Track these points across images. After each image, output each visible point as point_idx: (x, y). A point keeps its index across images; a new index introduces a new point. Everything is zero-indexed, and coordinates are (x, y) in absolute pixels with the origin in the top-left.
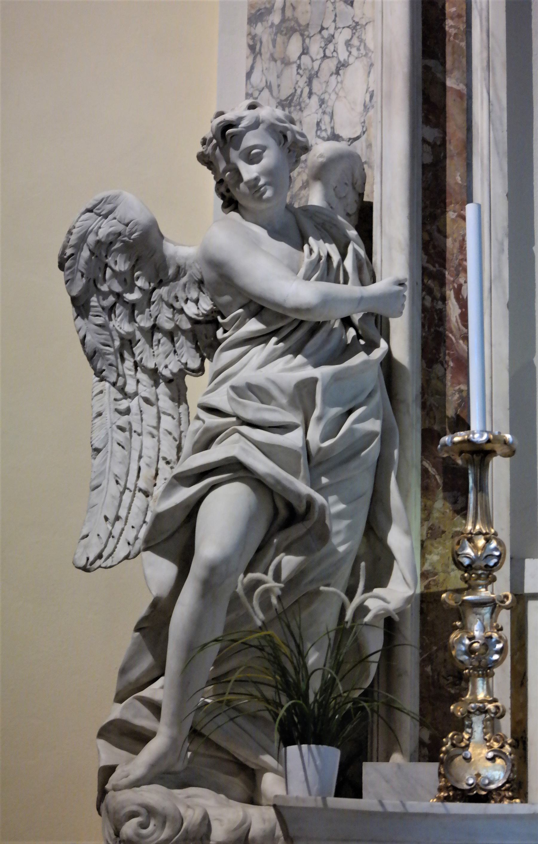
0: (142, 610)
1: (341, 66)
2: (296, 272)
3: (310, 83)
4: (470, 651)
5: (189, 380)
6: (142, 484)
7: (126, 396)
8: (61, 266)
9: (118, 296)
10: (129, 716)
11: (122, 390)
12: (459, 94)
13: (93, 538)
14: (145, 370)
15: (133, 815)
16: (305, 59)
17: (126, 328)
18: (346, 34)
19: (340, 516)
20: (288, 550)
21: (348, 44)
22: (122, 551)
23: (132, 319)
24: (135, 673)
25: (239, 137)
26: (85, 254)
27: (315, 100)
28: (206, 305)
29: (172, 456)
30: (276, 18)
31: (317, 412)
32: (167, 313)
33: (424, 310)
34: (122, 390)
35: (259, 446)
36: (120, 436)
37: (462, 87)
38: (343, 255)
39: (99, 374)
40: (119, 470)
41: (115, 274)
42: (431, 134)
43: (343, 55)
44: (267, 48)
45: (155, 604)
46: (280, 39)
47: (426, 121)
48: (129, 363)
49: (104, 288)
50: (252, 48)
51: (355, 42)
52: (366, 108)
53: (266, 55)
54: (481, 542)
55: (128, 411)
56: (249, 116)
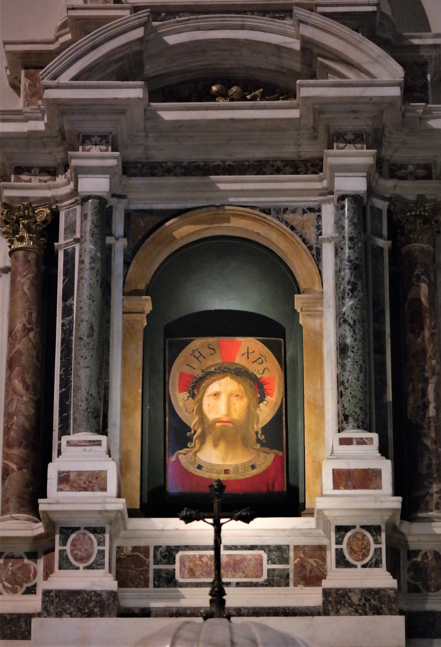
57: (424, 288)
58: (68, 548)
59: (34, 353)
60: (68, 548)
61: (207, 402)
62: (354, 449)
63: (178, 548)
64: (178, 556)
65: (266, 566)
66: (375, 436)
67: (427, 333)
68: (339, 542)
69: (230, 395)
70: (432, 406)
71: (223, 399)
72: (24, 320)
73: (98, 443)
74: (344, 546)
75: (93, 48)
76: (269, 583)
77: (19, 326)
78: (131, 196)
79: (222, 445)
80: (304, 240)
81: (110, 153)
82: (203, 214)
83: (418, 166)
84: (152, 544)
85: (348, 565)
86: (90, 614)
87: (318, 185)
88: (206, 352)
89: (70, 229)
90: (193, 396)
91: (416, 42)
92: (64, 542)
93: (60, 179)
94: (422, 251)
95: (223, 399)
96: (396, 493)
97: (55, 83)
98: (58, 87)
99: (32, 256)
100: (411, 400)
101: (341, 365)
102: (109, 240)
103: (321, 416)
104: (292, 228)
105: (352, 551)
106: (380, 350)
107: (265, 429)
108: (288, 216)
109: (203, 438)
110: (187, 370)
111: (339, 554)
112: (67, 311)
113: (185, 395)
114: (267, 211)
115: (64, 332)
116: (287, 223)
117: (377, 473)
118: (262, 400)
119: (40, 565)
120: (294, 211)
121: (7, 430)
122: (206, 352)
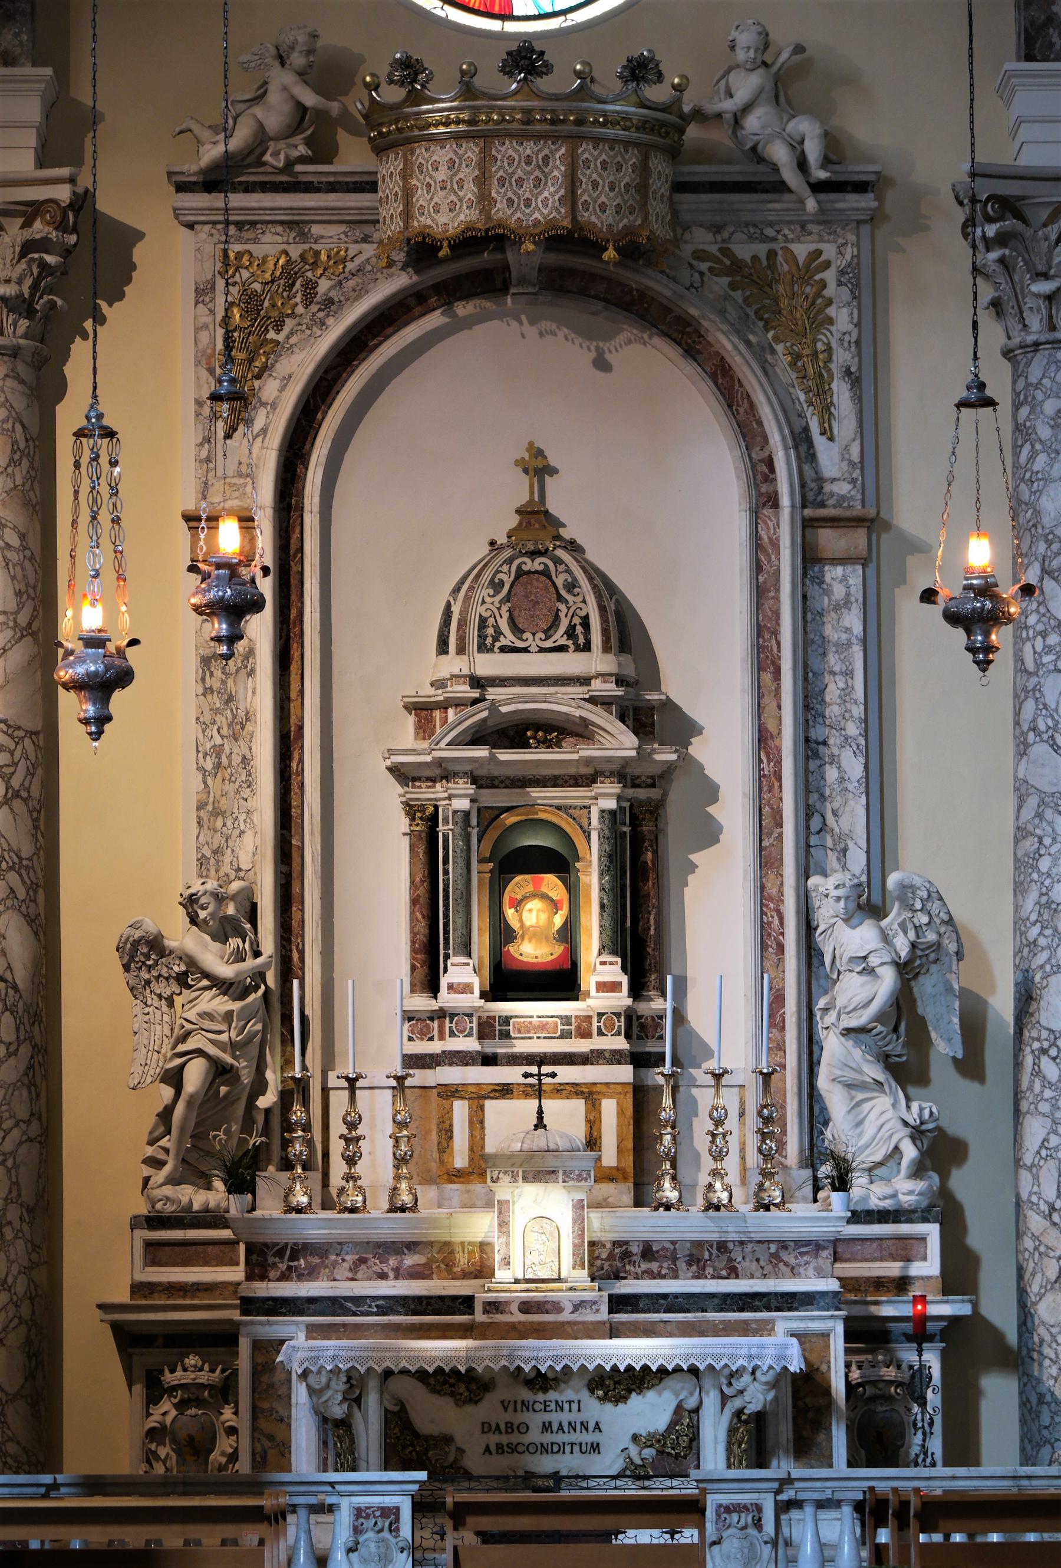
0: (160, 1109)
1: (242, 832)
2: (223, 958)
3: (227, 841)
4: (295, 1155)
5: (175, 997)
6: (156, 1048)
7: (147, 1006)
8: (118, 950)
9: (143, 963)
10: (155, 1155)
11: (145, 1003)
12: (298, 847)
13: (136, 1074)
14: (155, 994)
15: (161, 1200)
16: (225, 829)
17: (147, 976)
18: (244, 816)
19: (245, 1067)
20: (223, 1084)
21: (245, 821)
22: (149, 1080)
23: (149, 972)
24: (156, 1134)
25: (197, 901)
26: (129, 946)
27: (229, 851)
28: (183, 968)
29: (169, 1034)
30: (210, 808)
31: (234, 1025)
32: (165, 969)
33: (282, 956)
34: (145, 1003)
35: (212, 1041)
36: (146, 1026)
37: (299, 844)
38: (244, 942)
39: (135, 996)
40: (146, 1042)
41: (142, 954)
42: (285, 869)
43: (242, 827)
44: (206, 824)
45: (166, 1107)
46: (212, 819)
47: (283, 862)
48: (148, 991)
49: (137, 959)
50: (199, 823)
51: (248, 820)
52: (254, 855)
53: (206, 827)
54: (299, 1114)
55: (148, 1013)
56: (202, 888)
57: (650, 854)
58: (453, 1025)
59: (427, 895)
60: (453, 1025)
61: (525, 914)
62: (608, 967)
63: (511, 1017)
64: (511, 1021)
65: (560, 1027)
66: (619, 960)
67: (650, 883)
68: (599, 1022)
69: (538, 911)
70: (652, 928)
71: (534, 913)
72: (421, 875)
73: (468, 964)
74: (601, 1024)
75: (459, 724)
76: (561, 1037)
77: (418, 879)
78: (480, 799)
79: (534, 941)
80: (581, 828)
81: (469, 786)
82: (521, 810)
83: (648, 777)
84: (497, 1015)
85: (604, 1035)
86: (467, 1065)
87: (589, 794)
88: (523, 883)
89: (446, 821)
90: (517, 911)
91: (648, 697)
92: (451, 1023)
93: (438, 785)
94: (649, 831)
95: (534, 913)
96: (629, 997)
97: (438, 747)
98: (440, 749)
99: (424, 835)
100: (641, 924)
101: (601, 916)
102: (469, 829)
103: (590, 936)
104: (574, 819)
105: (606, 1027)
106: (624, 897)
107: (558, 931)
108: (572, 811)
109: (523, 937)
110: (513, 895)
111: (599, 1028)
112: (446, 872)
113: (512, 910)
114: (559, 808)
115: (444, 884)
116: (571, 816)
117: (620, 984)
118: (556, 913)
119: (436, 1024)
120: (575, 808)
121: (413, 943)
122: (523, 883)
